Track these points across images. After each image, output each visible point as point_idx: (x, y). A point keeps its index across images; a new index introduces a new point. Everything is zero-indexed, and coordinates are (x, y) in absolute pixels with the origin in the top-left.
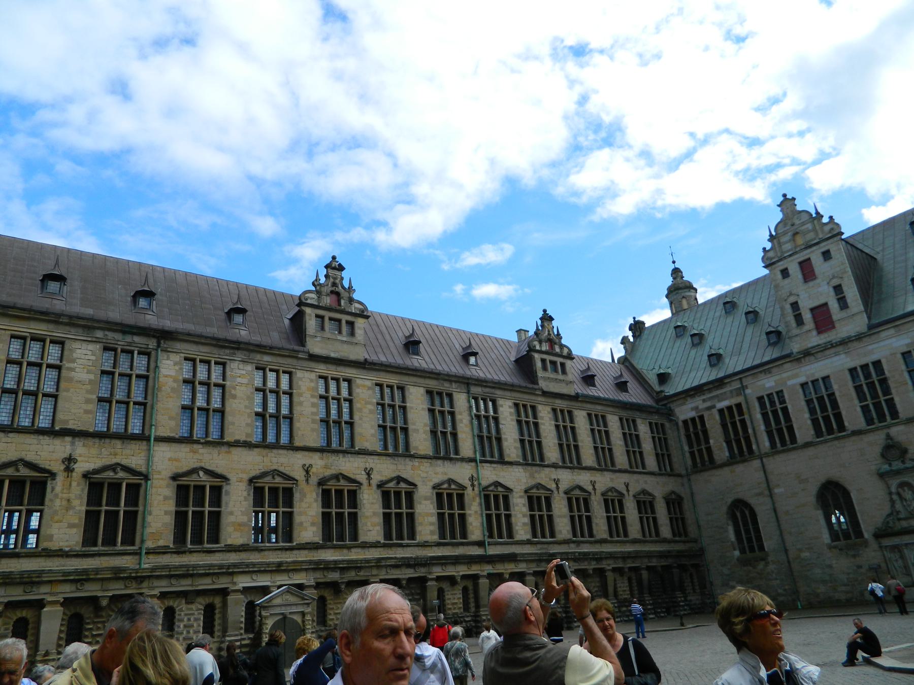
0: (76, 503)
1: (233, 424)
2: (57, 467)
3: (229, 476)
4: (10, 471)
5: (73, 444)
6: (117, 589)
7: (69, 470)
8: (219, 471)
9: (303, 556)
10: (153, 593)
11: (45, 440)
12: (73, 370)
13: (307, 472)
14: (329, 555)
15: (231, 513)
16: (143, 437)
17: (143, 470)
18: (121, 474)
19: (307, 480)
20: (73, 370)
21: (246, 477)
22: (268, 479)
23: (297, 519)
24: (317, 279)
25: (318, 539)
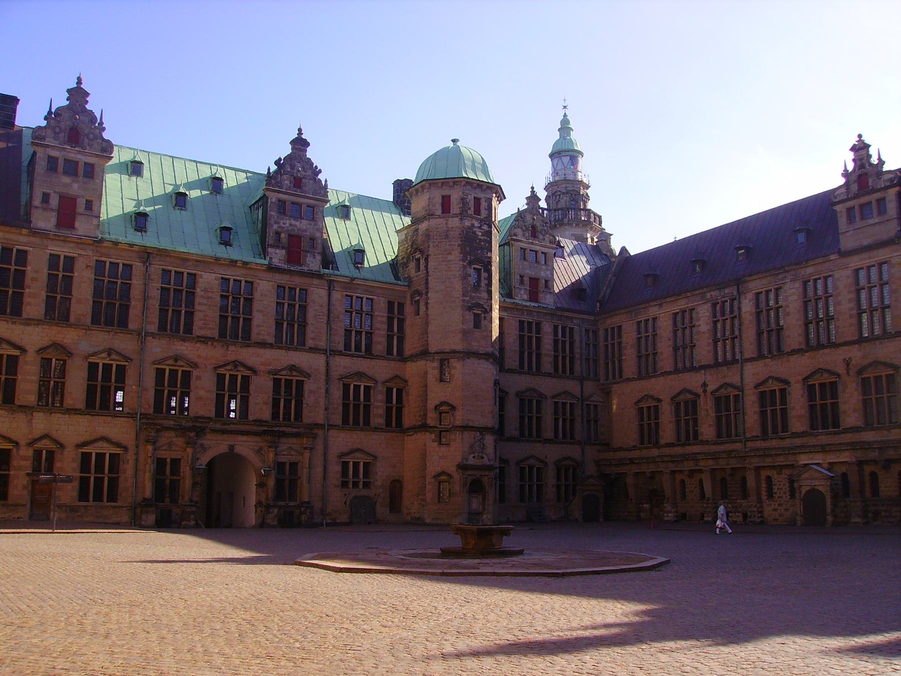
0: (710, 411)
1: (789, 337)
2: (700, 391)
3: (790, 380)
4: (682, 397)
5: (705, 374)
6: (734, 463)
7: (705, 391)
8: (783, 377)
9: (847, 438)
10: (751, 467)
11: (693, 374)
12: (699, 325)
13: (848, 365)
14: (869, 436)
15: (794, 408)
16: (734, 361)
17: (739, 384)
18: (730, 389)
19: (848, 373)
20: (699, 325)
21: (800, 378)
22: (818, 376)
23: (842, 407)
24: (846, 170)
25: (860, 424)
